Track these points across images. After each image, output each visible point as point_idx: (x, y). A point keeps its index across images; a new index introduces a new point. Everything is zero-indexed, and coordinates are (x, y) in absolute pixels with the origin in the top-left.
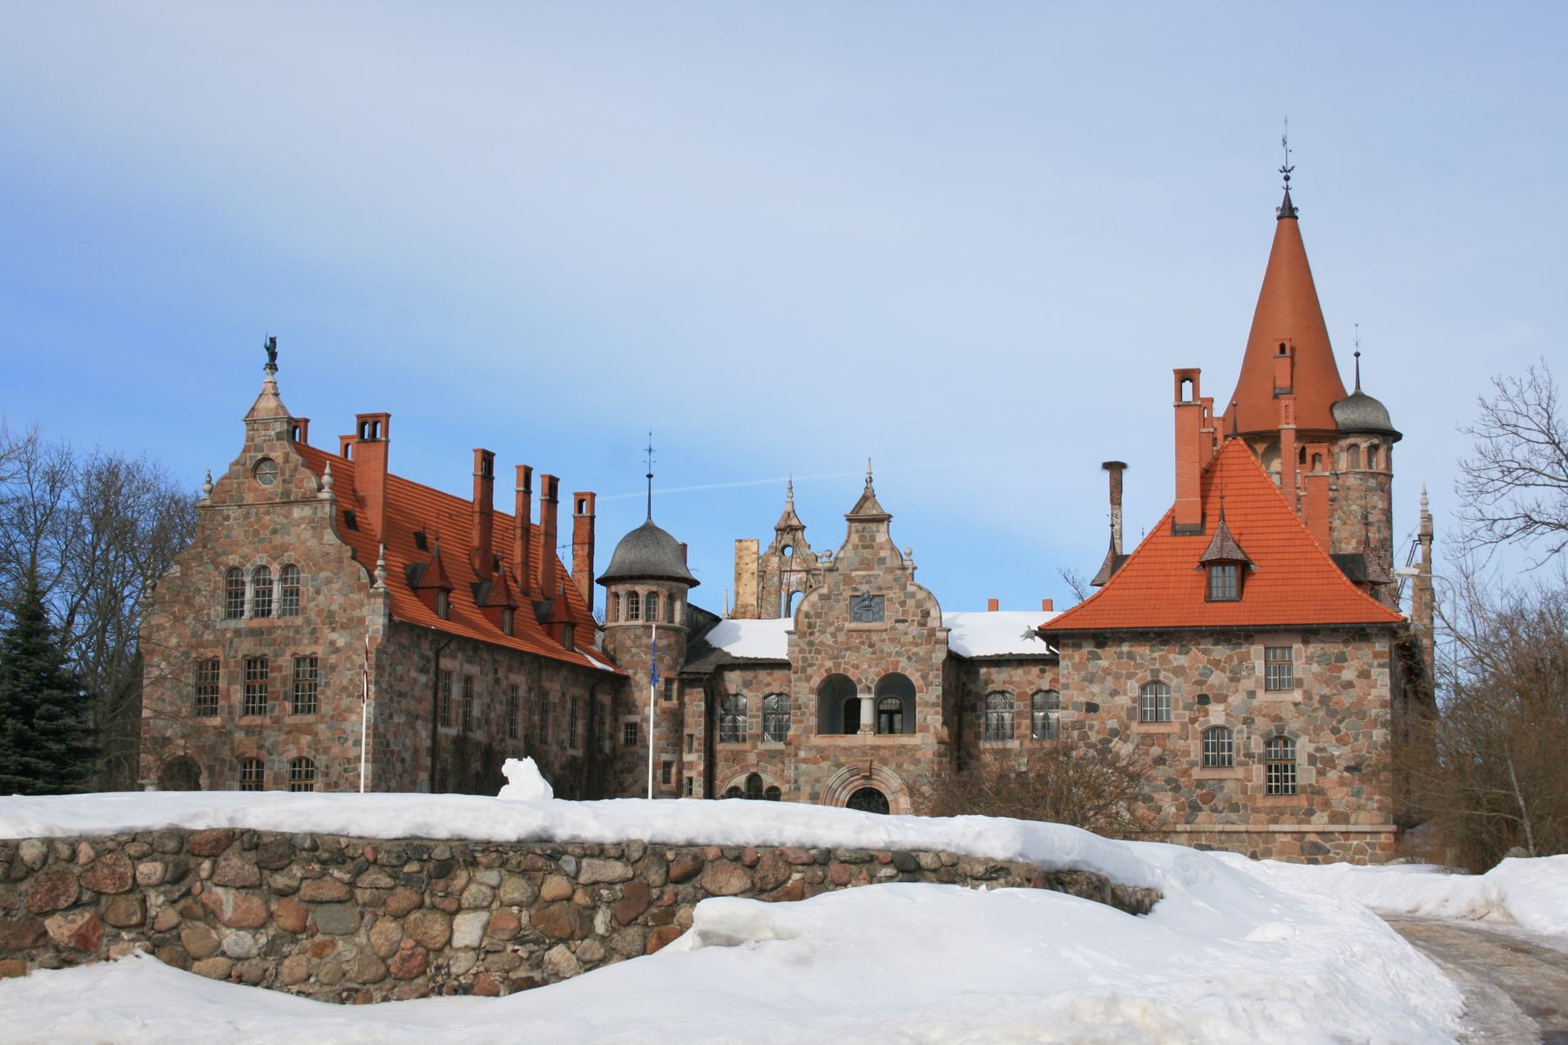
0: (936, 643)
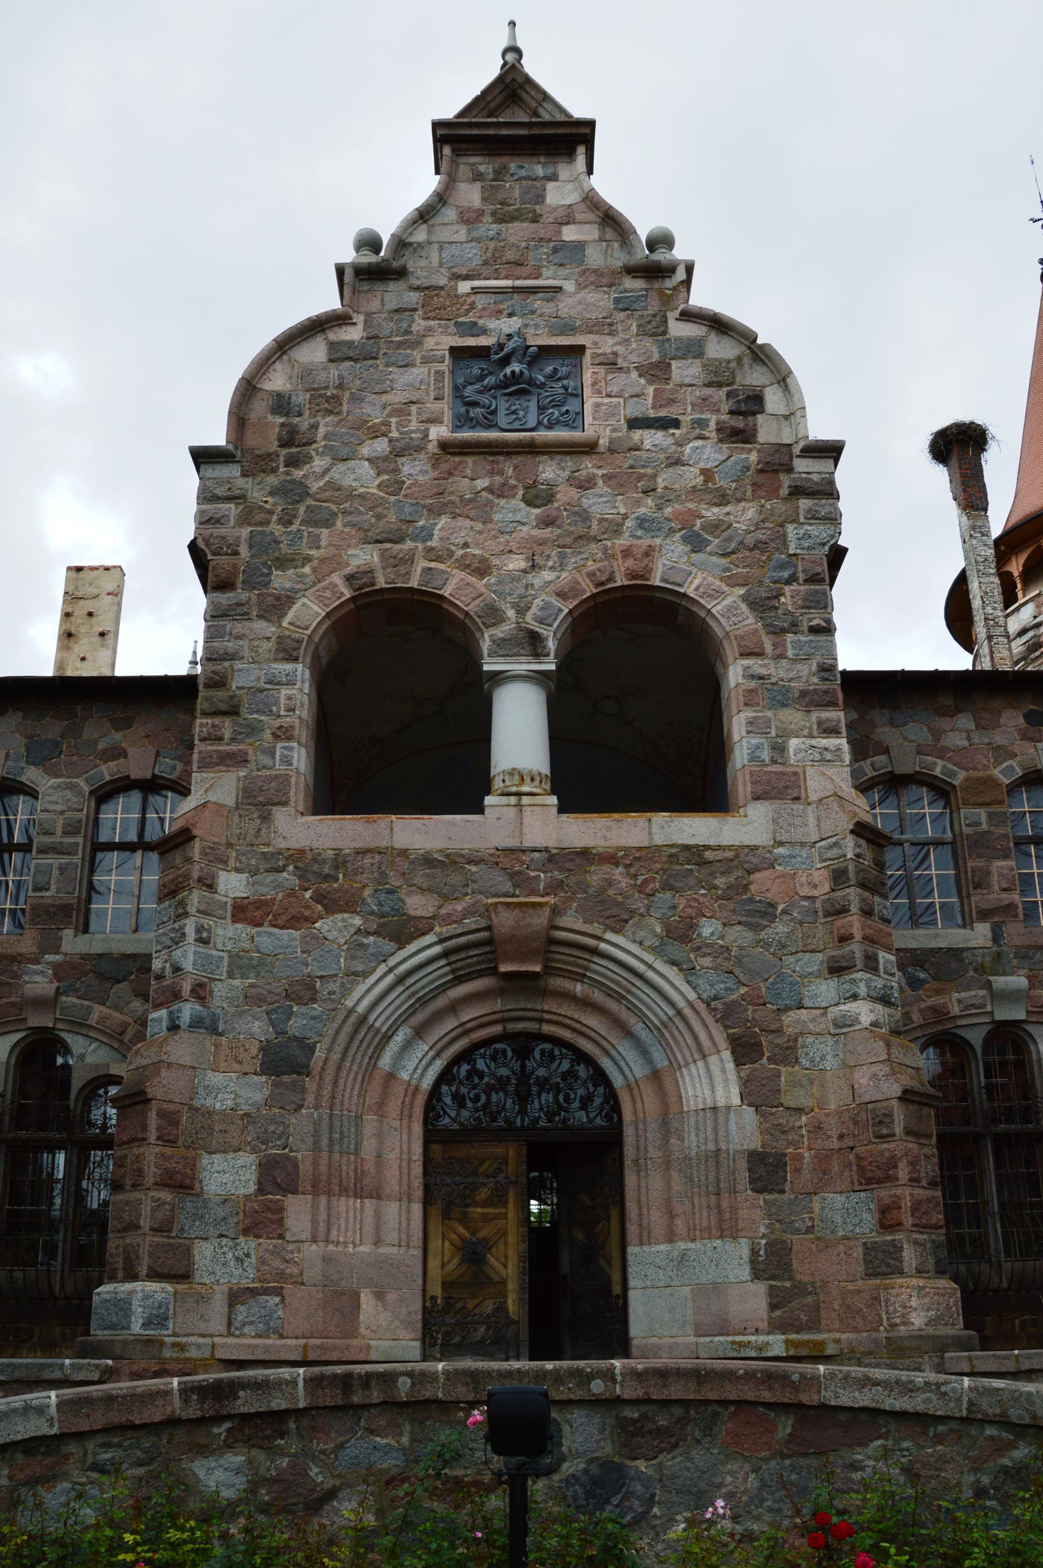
0: (798, 491)
